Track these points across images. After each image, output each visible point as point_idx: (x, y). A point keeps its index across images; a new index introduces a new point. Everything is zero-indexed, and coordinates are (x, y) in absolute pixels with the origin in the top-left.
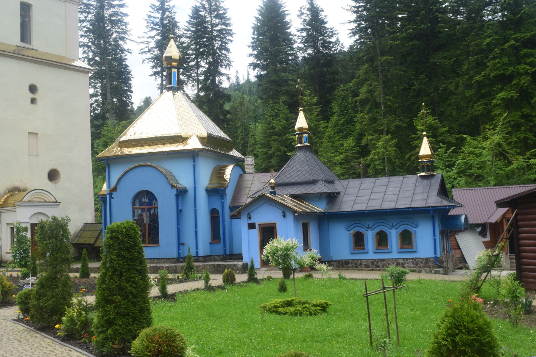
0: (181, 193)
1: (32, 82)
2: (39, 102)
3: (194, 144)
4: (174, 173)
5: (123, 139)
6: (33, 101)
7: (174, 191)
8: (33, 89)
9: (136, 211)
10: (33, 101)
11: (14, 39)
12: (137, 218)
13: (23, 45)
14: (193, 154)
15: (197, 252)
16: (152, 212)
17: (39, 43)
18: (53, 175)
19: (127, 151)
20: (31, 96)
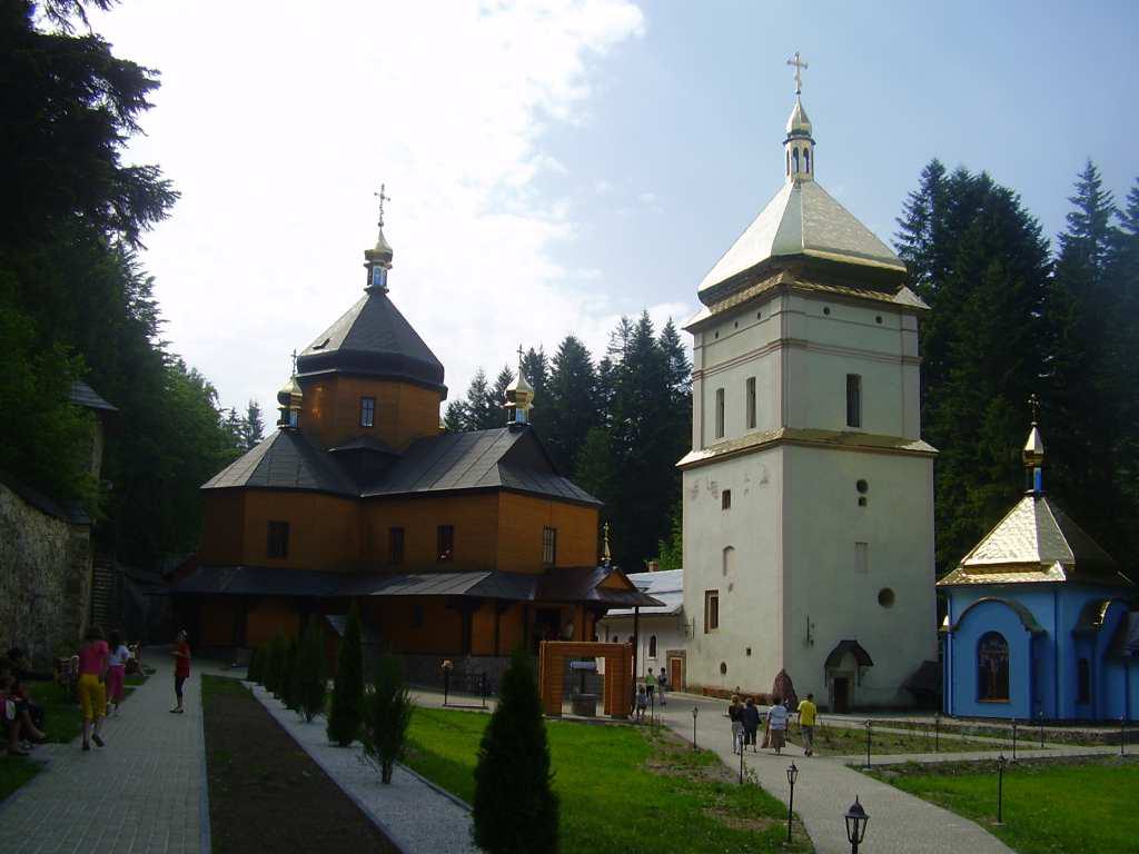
0: (1038, 638)
1: (860, 478)
2: (868, 504)
3: (1057, 573)
4: (1029, 608)
5: (969, 562)
6: (862, 502)
7: (1029, 635)
8: (862, 486)
9: (983, 656)
10: (862, 502)
11: (839, 424)
12: (983, 665)
13: (849, 429)
14: (1052, 588)
15: (1057, 715)
16: (1002, 658)
17: (871, 425)
18: (885, 597)
19: (973, 578)
20: (859, 495)
